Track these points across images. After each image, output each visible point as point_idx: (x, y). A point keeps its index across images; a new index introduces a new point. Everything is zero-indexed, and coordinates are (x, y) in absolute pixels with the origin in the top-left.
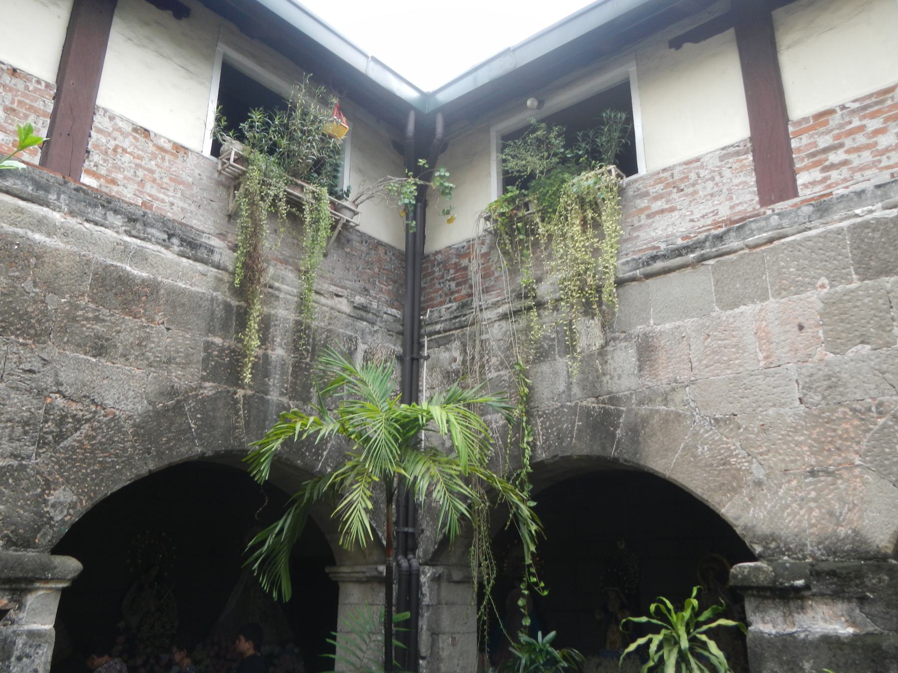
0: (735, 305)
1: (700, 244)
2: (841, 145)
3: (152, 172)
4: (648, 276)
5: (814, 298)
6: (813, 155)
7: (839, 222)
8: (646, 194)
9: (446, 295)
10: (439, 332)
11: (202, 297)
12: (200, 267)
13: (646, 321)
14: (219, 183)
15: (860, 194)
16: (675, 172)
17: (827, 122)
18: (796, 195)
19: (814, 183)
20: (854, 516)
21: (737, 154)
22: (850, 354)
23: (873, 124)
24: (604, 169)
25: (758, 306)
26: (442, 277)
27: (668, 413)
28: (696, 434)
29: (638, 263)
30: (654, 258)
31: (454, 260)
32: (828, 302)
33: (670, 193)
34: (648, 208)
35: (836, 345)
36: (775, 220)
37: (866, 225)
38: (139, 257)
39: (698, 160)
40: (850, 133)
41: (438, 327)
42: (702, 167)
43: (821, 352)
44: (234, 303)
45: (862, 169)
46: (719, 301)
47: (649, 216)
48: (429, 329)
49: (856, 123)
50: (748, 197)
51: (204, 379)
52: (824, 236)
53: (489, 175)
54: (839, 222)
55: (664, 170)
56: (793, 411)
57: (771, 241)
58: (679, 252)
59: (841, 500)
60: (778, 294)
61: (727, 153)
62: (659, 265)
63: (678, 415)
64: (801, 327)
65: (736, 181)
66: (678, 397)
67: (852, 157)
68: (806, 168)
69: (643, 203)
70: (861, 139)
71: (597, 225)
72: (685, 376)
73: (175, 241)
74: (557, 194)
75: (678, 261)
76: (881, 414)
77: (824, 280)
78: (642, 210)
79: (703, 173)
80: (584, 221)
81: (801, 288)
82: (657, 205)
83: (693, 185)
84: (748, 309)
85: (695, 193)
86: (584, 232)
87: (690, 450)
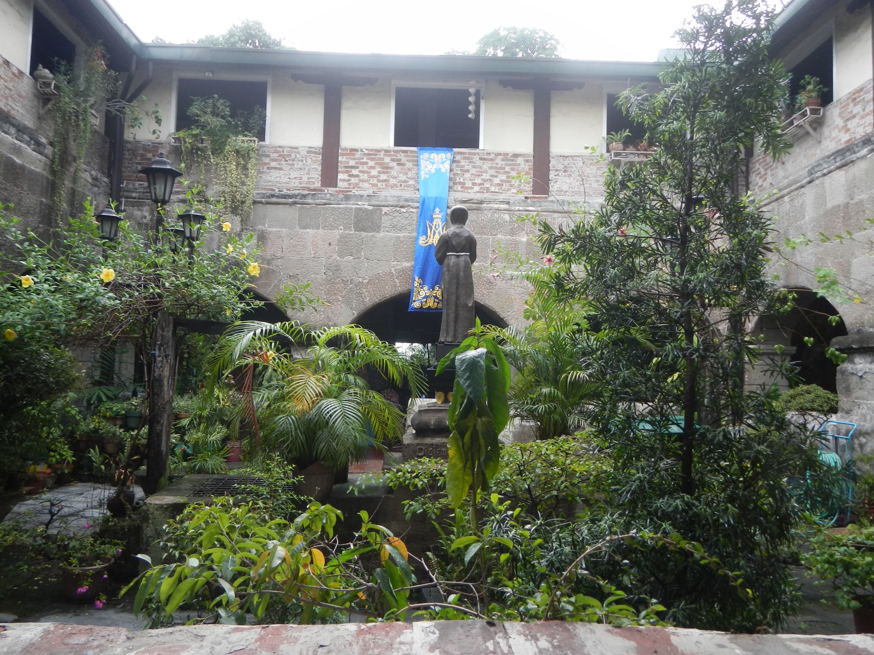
0: (305, 228)
1: (294, 196)
2: (358, 168)
3: (10, 90)
4: (268, 203)
5: (337, 233)
6: (346, 167)
7: (352, 205)
8: (268, 156)
9: (134, 172)
10: (134, 198)
11: (36, 173)
12: (39, 156)
13: (264, 224)
14: (35, 96)
15: (362, 196)
16: (285, 150)
17: (354, 155)
18: (336, 186)
19: (344, 180)
20: (335, 318)
21: (315, 153)
22: (345, 259)
23: (371, 163)
24: (252, 139)
25: (315, 231)
26: (131, 160)
27: (269, 269)
28: (280, 280)
29: (264, 196)
30: (273, 196)
31: (141, 152)
32: (342, 237)
33: (281, 160)
34: (269, 164)
35: (341, 255)
36: (328, 196)
37: (360, 209)
38: (18, 151)
39: (297, 148)
40: (363, 163)
41: (134, 195)
42: (298, 153)
43: (335, 256)
44: (50, 178)
45: (363, 181)
46: (299, 224)
47: (268, 168)
48: (126, 194)
49: (365, 160)
50: (317, 176)
51: (40, 223)
52: (346, 209)
53: (170, 103)
54: (352, 205)
55: (280, 147)
56: (321, 277)
57: (325, 204)
58: (285, 196)
59: (332, 312)
60: (323, 228)
61: (311, 151)
62: (274, 200)
63: (274, 271)
64: (330, 244)
65: (313, 166)
66: (274, 263)
67: (361, 174)
68: (343, 172)
69: (267, 160)
70: (365, 168)
71: (245, 168)
72: (279, 254)
73: (33, 142)
74: (224, 144)
75: (283, 200)
76: (351, 283)
77: (341, 227)
78: (265, 164)
79: (298, 156)
80: (238, 164)
81: (333, 228)
82: (273, 164)
83: (293, 160)
84: (311, 231)
85: (293, 165)
86: (237, 169)
87: (277, 286)
